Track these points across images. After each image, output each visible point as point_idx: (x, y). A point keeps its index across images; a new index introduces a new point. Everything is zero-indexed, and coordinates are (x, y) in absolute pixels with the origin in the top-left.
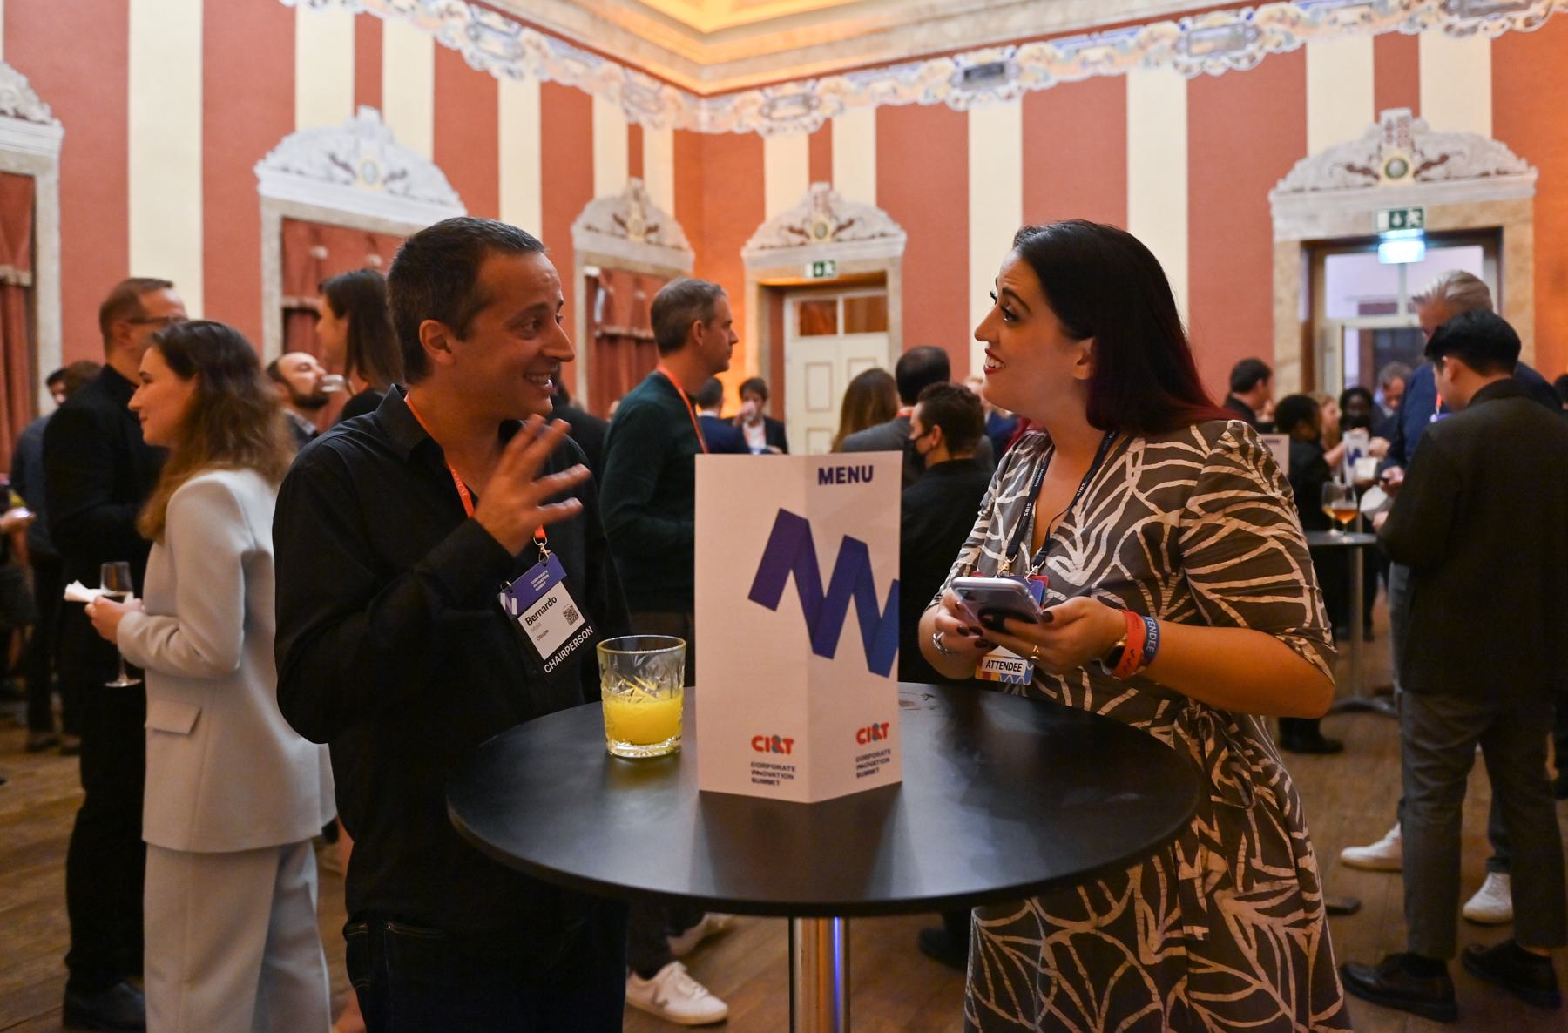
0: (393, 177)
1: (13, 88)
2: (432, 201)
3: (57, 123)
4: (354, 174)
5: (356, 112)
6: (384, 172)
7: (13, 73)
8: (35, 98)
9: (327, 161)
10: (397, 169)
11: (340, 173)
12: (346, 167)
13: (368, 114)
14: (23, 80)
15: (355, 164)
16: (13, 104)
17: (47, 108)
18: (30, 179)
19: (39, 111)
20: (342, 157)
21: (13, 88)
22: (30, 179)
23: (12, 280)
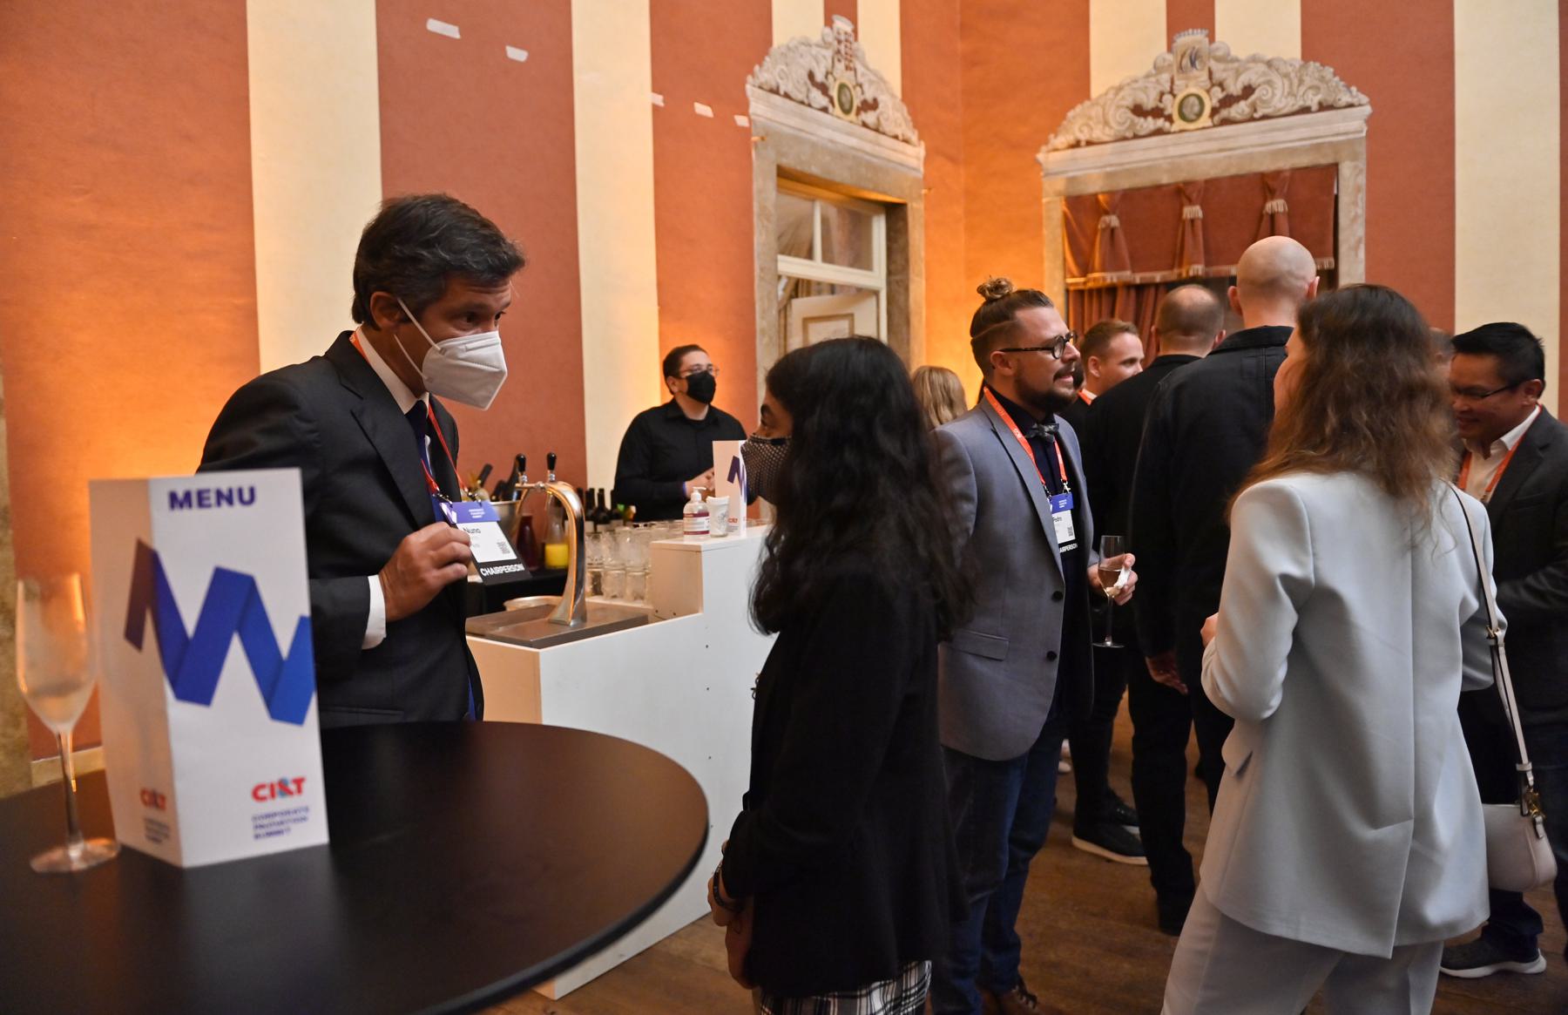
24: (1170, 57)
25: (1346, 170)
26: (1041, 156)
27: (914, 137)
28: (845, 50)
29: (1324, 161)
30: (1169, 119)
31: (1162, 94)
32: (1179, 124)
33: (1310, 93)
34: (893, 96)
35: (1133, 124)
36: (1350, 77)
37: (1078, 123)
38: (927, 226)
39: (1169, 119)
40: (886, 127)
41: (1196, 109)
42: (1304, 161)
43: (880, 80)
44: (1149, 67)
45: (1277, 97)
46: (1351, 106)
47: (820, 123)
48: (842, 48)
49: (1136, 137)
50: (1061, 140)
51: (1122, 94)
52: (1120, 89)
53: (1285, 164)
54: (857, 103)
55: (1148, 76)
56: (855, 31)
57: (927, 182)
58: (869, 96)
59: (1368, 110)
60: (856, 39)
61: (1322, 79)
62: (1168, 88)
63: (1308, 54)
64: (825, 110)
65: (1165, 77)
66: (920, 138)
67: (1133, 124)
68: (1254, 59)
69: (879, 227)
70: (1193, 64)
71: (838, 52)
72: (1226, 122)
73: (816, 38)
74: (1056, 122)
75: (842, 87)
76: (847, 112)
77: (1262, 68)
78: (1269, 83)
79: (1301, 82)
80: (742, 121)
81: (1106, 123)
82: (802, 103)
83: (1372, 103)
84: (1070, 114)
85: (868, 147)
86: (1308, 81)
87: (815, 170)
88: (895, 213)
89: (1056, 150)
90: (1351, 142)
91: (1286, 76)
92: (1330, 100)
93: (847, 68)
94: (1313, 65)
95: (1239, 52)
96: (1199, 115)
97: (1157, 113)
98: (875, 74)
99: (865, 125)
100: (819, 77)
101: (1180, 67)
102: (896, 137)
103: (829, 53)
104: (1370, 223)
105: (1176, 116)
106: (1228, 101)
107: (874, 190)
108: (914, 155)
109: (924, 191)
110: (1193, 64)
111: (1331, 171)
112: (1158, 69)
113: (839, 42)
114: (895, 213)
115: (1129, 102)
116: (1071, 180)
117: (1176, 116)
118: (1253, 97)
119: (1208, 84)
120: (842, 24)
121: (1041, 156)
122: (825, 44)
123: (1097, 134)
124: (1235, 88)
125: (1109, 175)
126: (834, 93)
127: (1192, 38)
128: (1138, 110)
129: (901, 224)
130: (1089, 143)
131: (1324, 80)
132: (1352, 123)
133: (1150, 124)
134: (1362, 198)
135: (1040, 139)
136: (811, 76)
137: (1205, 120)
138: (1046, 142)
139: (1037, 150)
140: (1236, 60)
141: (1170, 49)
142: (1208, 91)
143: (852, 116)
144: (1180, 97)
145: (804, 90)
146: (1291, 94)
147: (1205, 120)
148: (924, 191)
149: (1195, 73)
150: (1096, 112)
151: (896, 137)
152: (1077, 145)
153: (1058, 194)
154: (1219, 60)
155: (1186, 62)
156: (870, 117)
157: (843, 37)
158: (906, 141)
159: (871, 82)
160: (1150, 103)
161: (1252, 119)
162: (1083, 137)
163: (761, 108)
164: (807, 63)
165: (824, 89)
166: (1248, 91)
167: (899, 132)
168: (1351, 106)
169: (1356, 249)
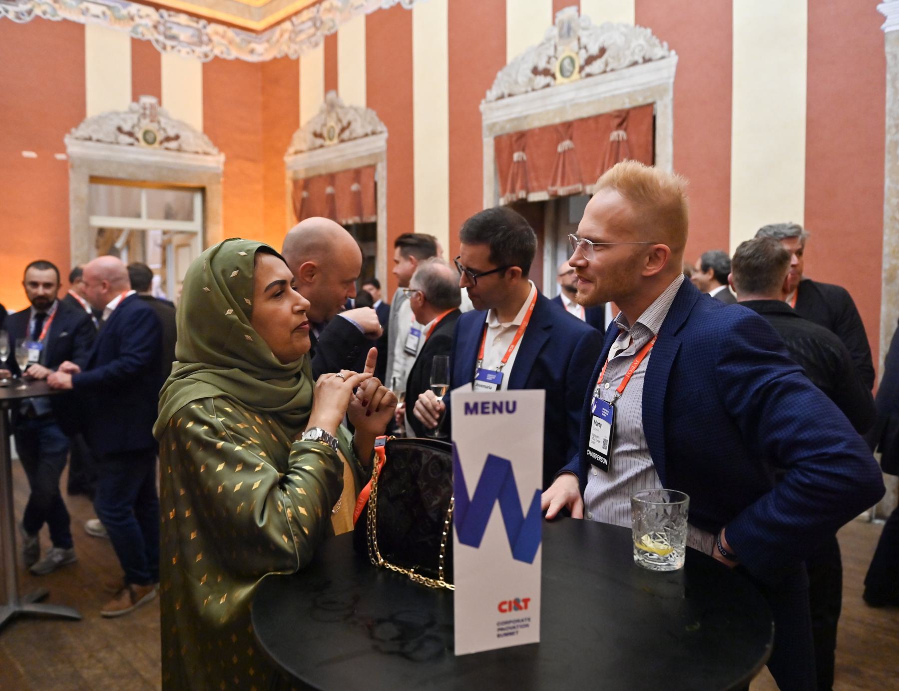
3: (673, 52)
7: (642, 29)
8: (657, 41)
14: (649, 31)
16: (642, 54)
19: (659, 51)
21: (642, 41)
22: (651, 106)
27: (215, 151)
29: (372, 162)
38: (225, 198)
40: (185, 147)
42: (366, 162)
43: (182, 124)
45: (358, 128)
48: (148, 112)
50: (291, 150)
57: (225, 174)
58: (172, 133)
59: (385, 135)
64: (132, 144)
68: (351, 107)
69: (198, 198)
75: (146, 133)
80: (60, 157)
87: (121, 175)
88: (203, 190)
112: (322, 112)
114: (203, 190)
116: (295, 172)
122: (132, 111)
125: (307, 170)
126: (140, 135)
128: (318, 135)
132: (380, 143)
133: (319, 142)
143: (156, 145)
151: (197, 153)
163: (74, 147)
164: (117, 122)
165: (131, 134)
166: (349, 124)
167: (200, 150)
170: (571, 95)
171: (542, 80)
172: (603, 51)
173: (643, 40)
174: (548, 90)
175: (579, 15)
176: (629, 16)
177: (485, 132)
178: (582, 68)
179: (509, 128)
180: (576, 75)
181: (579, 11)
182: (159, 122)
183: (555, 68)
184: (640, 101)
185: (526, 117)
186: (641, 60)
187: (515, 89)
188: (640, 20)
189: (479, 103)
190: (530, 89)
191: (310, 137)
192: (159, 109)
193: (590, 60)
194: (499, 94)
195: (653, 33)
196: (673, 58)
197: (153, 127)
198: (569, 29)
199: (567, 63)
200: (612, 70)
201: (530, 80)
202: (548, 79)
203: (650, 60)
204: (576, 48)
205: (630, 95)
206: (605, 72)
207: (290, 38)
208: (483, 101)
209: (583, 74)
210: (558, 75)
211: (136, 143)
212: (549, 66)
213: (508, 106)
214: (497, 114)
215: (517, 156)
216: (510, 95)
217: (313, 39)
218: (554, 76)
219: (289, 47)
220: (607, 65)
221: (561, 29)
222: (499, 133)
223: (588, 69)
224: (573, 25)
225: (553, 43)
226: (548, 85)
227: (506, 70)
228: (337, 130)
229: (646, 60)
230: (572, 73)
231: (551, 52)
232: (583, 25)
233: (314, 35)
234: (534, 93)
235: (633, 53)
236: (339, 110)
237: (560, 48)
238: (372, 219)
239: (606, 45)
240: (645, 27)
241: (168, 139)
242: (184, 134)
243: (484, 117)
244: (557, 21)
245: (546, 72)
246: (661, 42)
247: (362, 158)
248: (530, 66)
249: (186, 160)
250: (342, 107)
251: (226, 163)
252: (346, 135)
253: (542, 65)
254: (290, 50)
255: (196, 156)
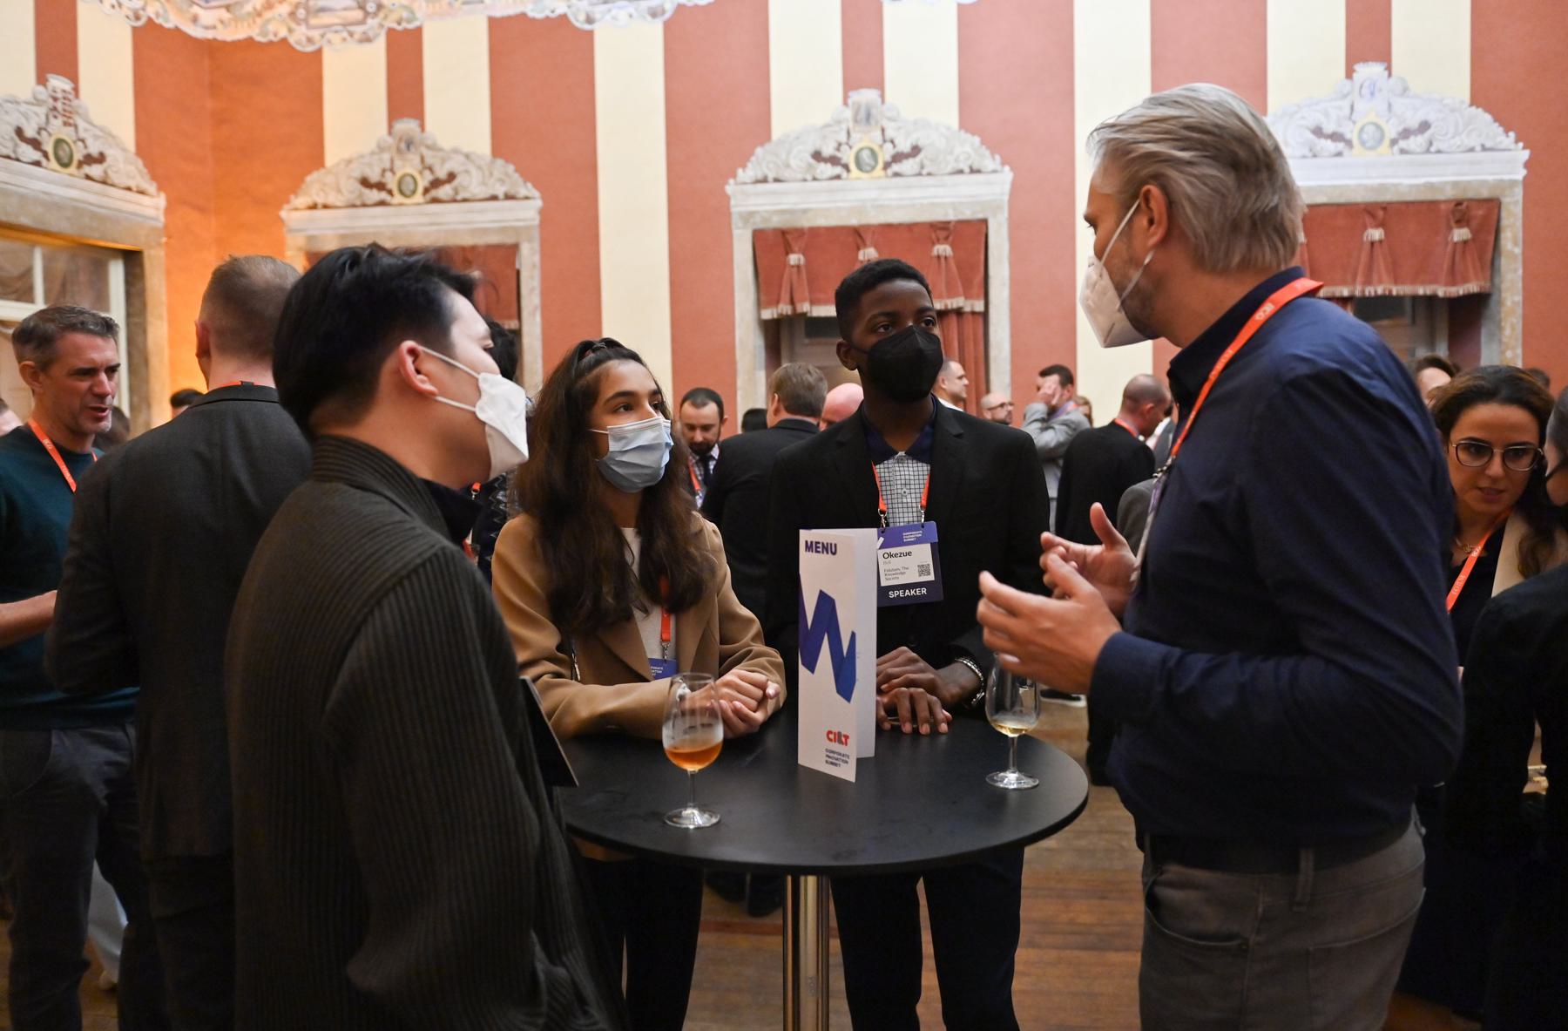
0: (1406, 134)
1: (968, 148)
2: (1472, 150)
3: (1007, 168)
4: (1349, 143)
5: (1349, 74)
6: (1391, 131)
7: (968, 136)
8: (987, 153)
9: (1311, 136)
10: (1413, 123)
11: (1330, 146)
12: (1336, 137)
13: (1369, 71)
14: (977, 140)
15: (1351, 132)
17: (998, 157)
18: (985, 222)
19: (989, 162)
20: (1329, 128)
21: (968, 148)
23: (967, 309)
24: (390, 140)
25: (525, 250)
26: (283, 214)
27: (152, 188)
28: (64, 109)
29: (509, 240)
30: (390, 192)
31: (384, 171)
32: (398, 198)
33: (498, 185)
34: (124, 150)
35: (361, 195)
36: (527, 176)
37: (316, 187)
38: (168, 273)
39: (390, 192)
40: (114, 178)
41: (412, 187)
42: (494, 239)
43: (108, 135)
44: (373, 146)
45: (472, 184)
46: (527, 198)
47: (30, 176)
48: (59, 105)
49: (364, 205)
50: (301, 201)
51: (353, 166)
52: (349, 162)
53: (481, 241)
54: (78, 156)
55: (373, 153)
56: (76, 90)
57: (167, 230)
58: (94, 150)
59: (539, 203)
60: (77, 95)
61: (507, 174)
62: (388, 165)
63: (497, 151)
64: (37, 164)
65: (386, 156)
66: (160, 188)
67: (361, 195)
68: (456, 151)
69: (116, 273)
70: (408, 147)
71: (55, 109)
72: (435, 200)
73: (28, 96)
74: (296, 186)
75: (59, 143)
76: (65, 165)
77: (461, 159)
78: (467, 172)
79: (491, 174)
81: (339, 191)
82: (8, 157)
83: (543, 198)
84: (309, 179)
85: (92, 198)
86: (497, 174)
87: (24, 220)
88: (132, 259)
89: (296, 209)
90: (528, 228)
91: (479, 168)
92: (512, 192)
93: (65, 124)
94: (500, 162)
95: (446, 143)
96: (414, 192)
97: (380, 186)
98: (102, 129)
99: (88, 177)
100: (30, 132)
101: (399, 151)
102: (129, 189)
103: (42, 111)
104: (545, 294)
105: (395, 191)
106: (436, 183)
107: (102, 239)
108: (153, 206)
109: (164, 240)
110: (408, 147)
111: (512, 250)
112: (381, 149)
113: (55, 99)
114: (132, 259)
115: (357, 174)
116: (311, 238)
117: (395, 191)
118: (456, 183)
119: (420, 167)
120: (58, 83)
121: (283, 214)
123: (332, 199)
124: (442, 174)
125: (343, 237)
126: (49, 148)
127: (407, 126)
129: (138, 270)
130: (325, 207)
131: (505, 176)
132: (527, 212)
133: (375, 195)
134: (537, 273)
135: (281, 199)
136: (19, 132)
137: (418, 197)
138: (288, 202)
139: (280, 208)
140: (440, 150)
141: (390, 133)
142: (421, 173)
143: (72, 169)
144: (399, 174)
145: (10, 145)
146: (484, 183)
147: (418, 197)
148: (164, 240)
149: (410, 156)
150: (330, 179)
151: (129, 189)
152: (314, 207)
153: (300, 249)
154: (428, 147)
155: (403, 146)
156: (96, 170)
157: (59, 95)
158: (142, 192)
159: (96, 137)
160: (374, 177)
161: (455, 201)
162: (320, 200)
164: (15, 119)
165: (35, 144)
166: (451, 177)
167: (132, 184)
168: (527, 198)
169: (534, 314)
170: (874, 194)
171: (827, 170)
172: (916, 150)
173: (969, 147)
174: (836, 183)
175: (883, 101)
176: (953, 119)
177: (736, 221)
178: (887, 165)
179: (776, 222)
180: (879, 171)
181: (882, 96)
182: (76, 126)
183: (848, 156)
184: (967, 214)
185: (805, 211)
186: (967, 170)
187: (786, 174)
188: (965, 124)
189: (726, 183)
190: (809, 177)
191: (351, 189)
192: (75, 103)
193: (898, 158)
194: (760, 176)
195: (983, 143)
196: (1007, 175)
197: (67, 134)
198: (868, 116)
199: (865, 155)
200: (929, 174)
201: (810, 166)
202: (838, 170)
203: (979, 171)
204: (879, 139)
205: (954, 206)
206: (920, 174)
207: (292, 14)
208: (731, 181)
209: (890, 171)
210: (853, 166)
211: (44, 162)
212: (839, 155)
213: (774, 193)
214: (758, 198)
215: (794, 259)
216: (777, 180)
217: (358, 30)
218: (846, 167)
219: (290, 30)
220: (922, 167)
221: (856, 113)
222: (761, 226)
223: (895, 168)
224: (874, 111)
225: (844, 127)
226: (838, 177)
227: (767, 146)
228: (422, 183)
229: (973, 171)
230: (873, 168)
231: (843, 138)
232: (889, 114)
233: (363, 22)
234: (816, 184)
235: (956, 160)
236: (427, 153)
237: (853, 135)
238: (513, 324)
239: (921, 144)
240: (973, 134)
241: (89, 160)
242: (109, 152)
243: (733, 202)
244: (850, 101)
245: (834, 161)
246: (993, 154)
247: (485, 231)
248: (811, 149)
249: (116, 200)
250: (433, 147)
251: (169, 211)
252: (444, 191)
253: (828, 151)
254: (299, 37)
255: (128, 195)
